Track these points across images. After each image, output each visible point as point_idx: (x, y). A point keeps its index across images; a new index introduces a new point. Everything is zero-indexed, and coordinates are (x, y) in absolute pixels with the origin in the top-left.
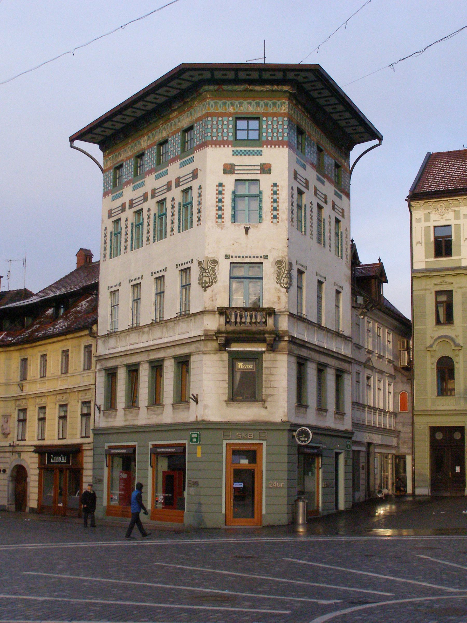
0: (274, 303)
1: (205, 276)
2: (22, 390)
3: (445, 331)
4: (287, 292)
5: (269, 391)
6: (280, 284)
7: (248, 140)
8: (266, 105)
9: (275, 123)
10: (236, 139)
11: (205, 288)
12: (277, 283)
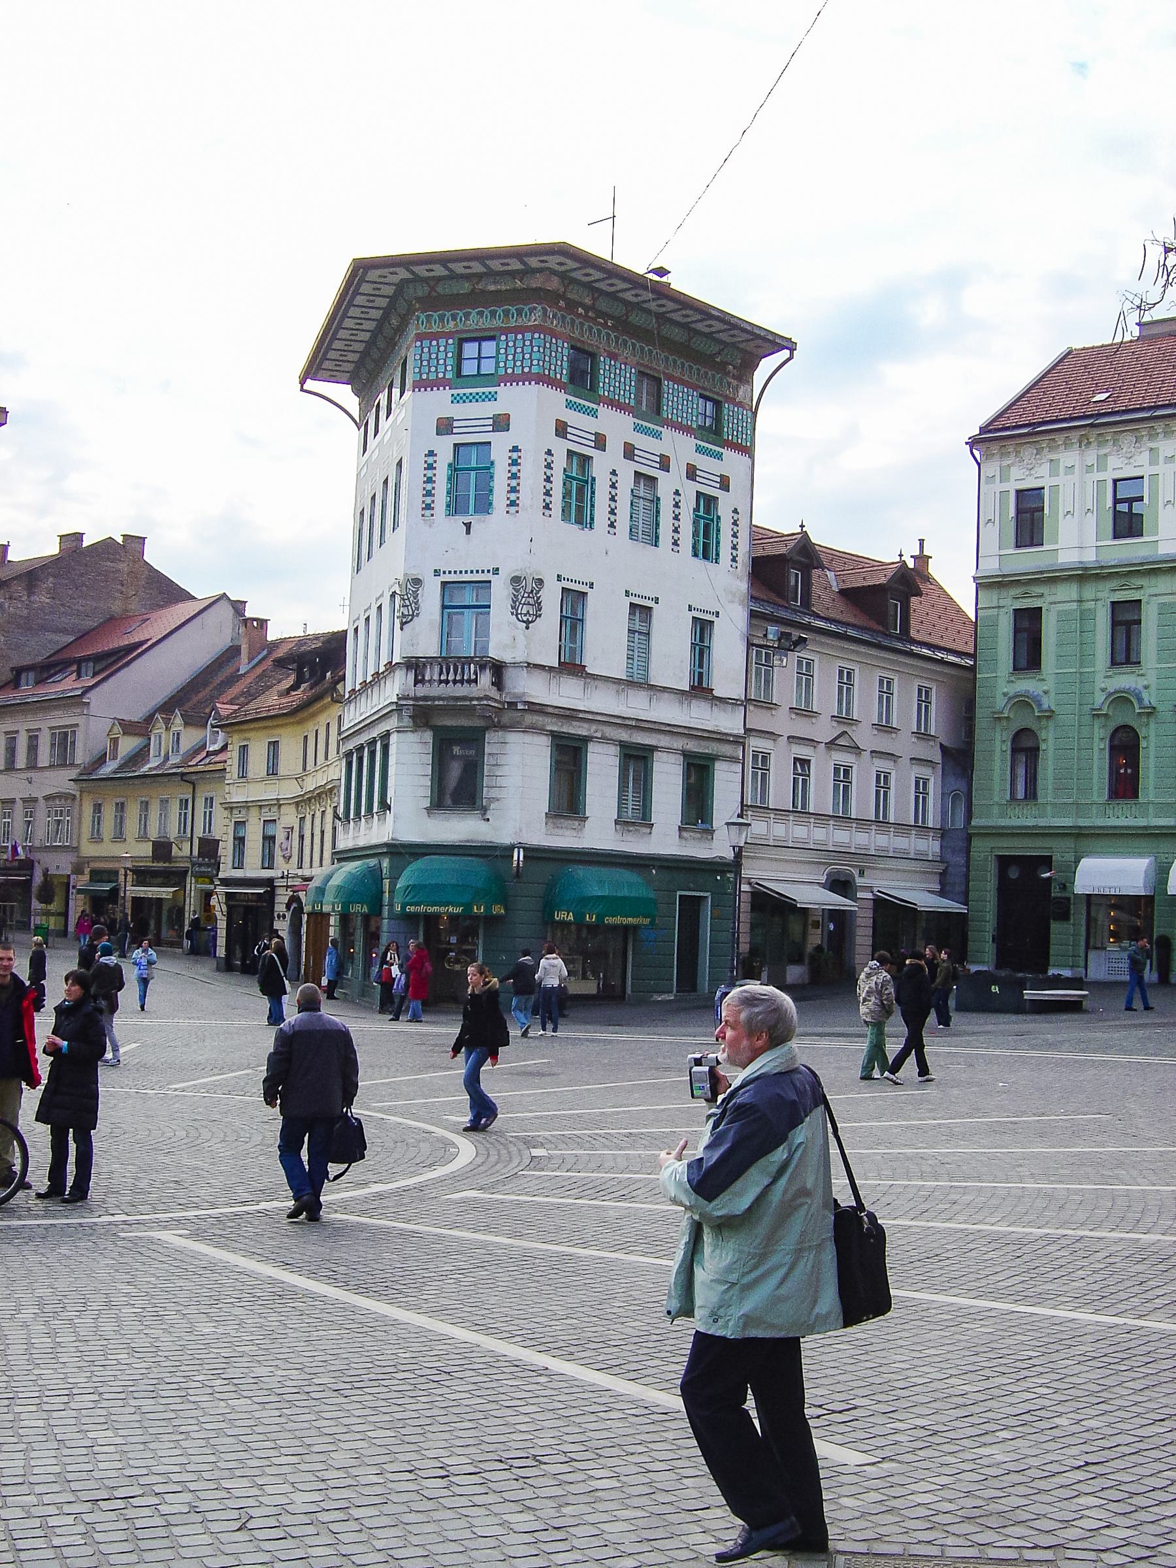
3: (1026, 685)
4: (527, 628)
5: (493, 793)
7: (479, 374)
9: (519, 344)
10: (459, 374)
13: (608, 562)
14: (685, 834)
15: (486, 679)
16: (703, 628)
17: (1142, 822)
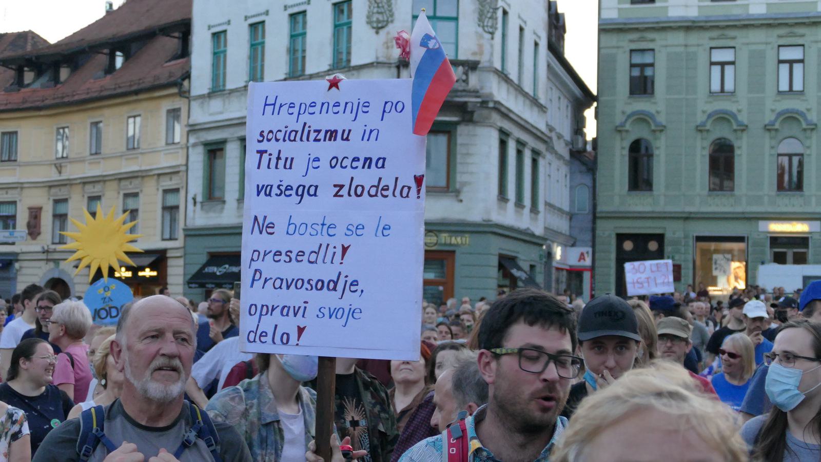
0: (474, 54)
1: (378, 13)
2: (60, 173)
3: (642, 105)
6: (483, 27)
11: (378, 30)
12: (479, 25)
17: (739, 209)
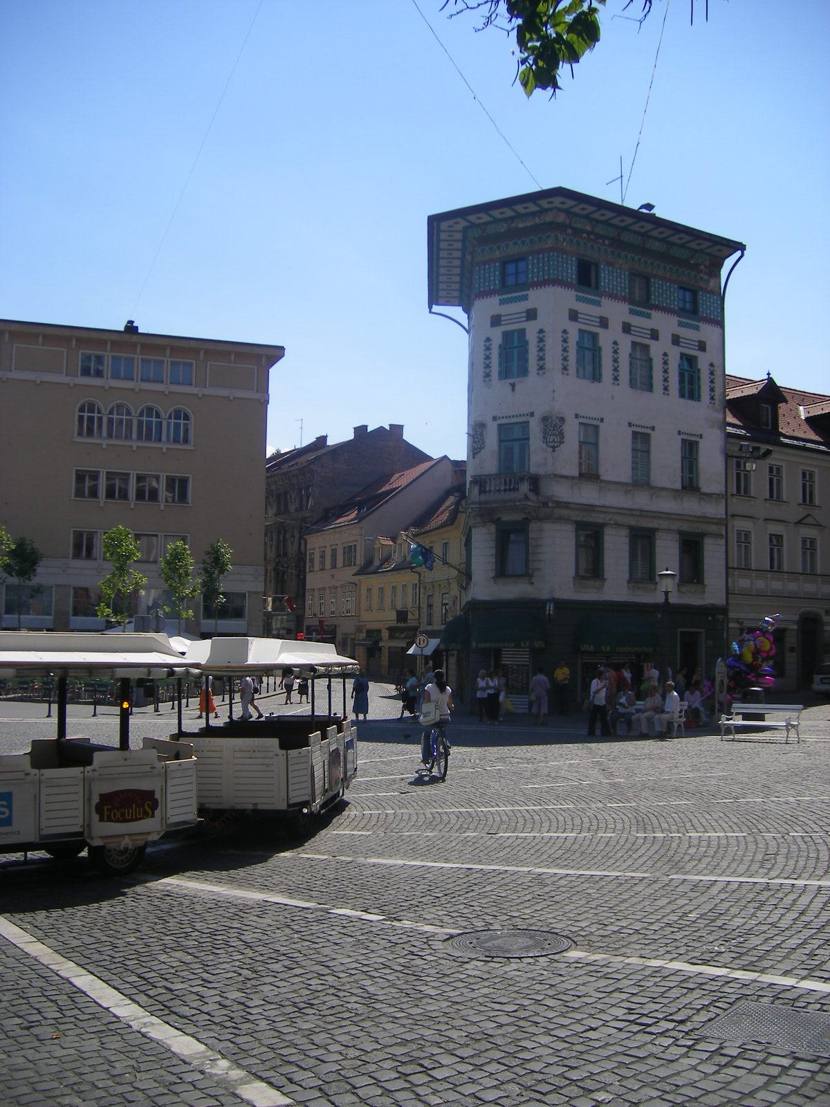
4: (554, 451)
8: (532, 242)
13: (614, 405)
14: (684, 589)
15: (525, 487)
16: (690, 449)
